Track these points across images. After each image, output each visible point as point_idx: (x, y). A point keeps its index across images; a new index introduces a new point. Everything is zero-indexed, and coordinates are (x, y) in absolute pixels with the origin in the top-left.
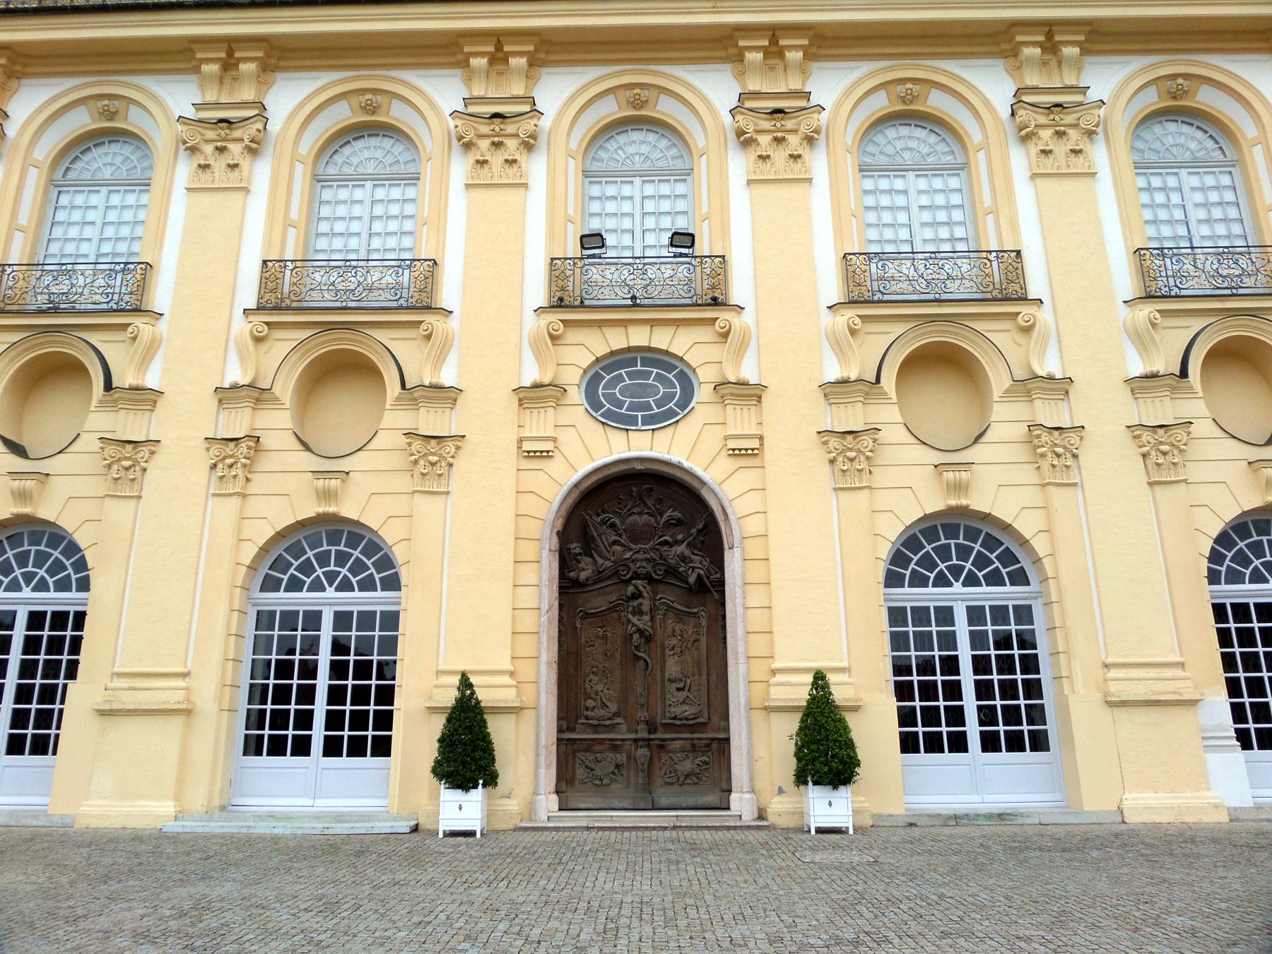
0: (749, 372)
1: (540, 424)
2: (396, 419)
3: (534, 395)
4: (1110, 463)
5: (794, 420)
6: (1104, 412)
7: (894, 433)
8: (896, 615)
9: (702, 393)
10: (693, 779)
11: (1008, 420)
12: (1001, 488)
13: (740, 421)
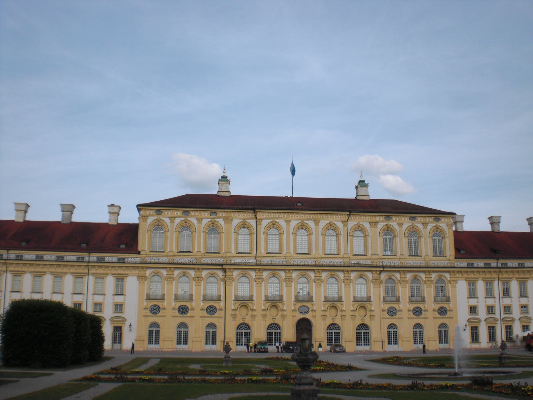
0: (314, 308)
1: (294, 313)
2: (280, 313)
3: (294, 310)
4: (348, 318)
5: (319, 314)
6: (348, 314)
8: (327, 333)
9: (310, 311)
11: (340, 314)
12: (338, 321)
13: (314, 314)
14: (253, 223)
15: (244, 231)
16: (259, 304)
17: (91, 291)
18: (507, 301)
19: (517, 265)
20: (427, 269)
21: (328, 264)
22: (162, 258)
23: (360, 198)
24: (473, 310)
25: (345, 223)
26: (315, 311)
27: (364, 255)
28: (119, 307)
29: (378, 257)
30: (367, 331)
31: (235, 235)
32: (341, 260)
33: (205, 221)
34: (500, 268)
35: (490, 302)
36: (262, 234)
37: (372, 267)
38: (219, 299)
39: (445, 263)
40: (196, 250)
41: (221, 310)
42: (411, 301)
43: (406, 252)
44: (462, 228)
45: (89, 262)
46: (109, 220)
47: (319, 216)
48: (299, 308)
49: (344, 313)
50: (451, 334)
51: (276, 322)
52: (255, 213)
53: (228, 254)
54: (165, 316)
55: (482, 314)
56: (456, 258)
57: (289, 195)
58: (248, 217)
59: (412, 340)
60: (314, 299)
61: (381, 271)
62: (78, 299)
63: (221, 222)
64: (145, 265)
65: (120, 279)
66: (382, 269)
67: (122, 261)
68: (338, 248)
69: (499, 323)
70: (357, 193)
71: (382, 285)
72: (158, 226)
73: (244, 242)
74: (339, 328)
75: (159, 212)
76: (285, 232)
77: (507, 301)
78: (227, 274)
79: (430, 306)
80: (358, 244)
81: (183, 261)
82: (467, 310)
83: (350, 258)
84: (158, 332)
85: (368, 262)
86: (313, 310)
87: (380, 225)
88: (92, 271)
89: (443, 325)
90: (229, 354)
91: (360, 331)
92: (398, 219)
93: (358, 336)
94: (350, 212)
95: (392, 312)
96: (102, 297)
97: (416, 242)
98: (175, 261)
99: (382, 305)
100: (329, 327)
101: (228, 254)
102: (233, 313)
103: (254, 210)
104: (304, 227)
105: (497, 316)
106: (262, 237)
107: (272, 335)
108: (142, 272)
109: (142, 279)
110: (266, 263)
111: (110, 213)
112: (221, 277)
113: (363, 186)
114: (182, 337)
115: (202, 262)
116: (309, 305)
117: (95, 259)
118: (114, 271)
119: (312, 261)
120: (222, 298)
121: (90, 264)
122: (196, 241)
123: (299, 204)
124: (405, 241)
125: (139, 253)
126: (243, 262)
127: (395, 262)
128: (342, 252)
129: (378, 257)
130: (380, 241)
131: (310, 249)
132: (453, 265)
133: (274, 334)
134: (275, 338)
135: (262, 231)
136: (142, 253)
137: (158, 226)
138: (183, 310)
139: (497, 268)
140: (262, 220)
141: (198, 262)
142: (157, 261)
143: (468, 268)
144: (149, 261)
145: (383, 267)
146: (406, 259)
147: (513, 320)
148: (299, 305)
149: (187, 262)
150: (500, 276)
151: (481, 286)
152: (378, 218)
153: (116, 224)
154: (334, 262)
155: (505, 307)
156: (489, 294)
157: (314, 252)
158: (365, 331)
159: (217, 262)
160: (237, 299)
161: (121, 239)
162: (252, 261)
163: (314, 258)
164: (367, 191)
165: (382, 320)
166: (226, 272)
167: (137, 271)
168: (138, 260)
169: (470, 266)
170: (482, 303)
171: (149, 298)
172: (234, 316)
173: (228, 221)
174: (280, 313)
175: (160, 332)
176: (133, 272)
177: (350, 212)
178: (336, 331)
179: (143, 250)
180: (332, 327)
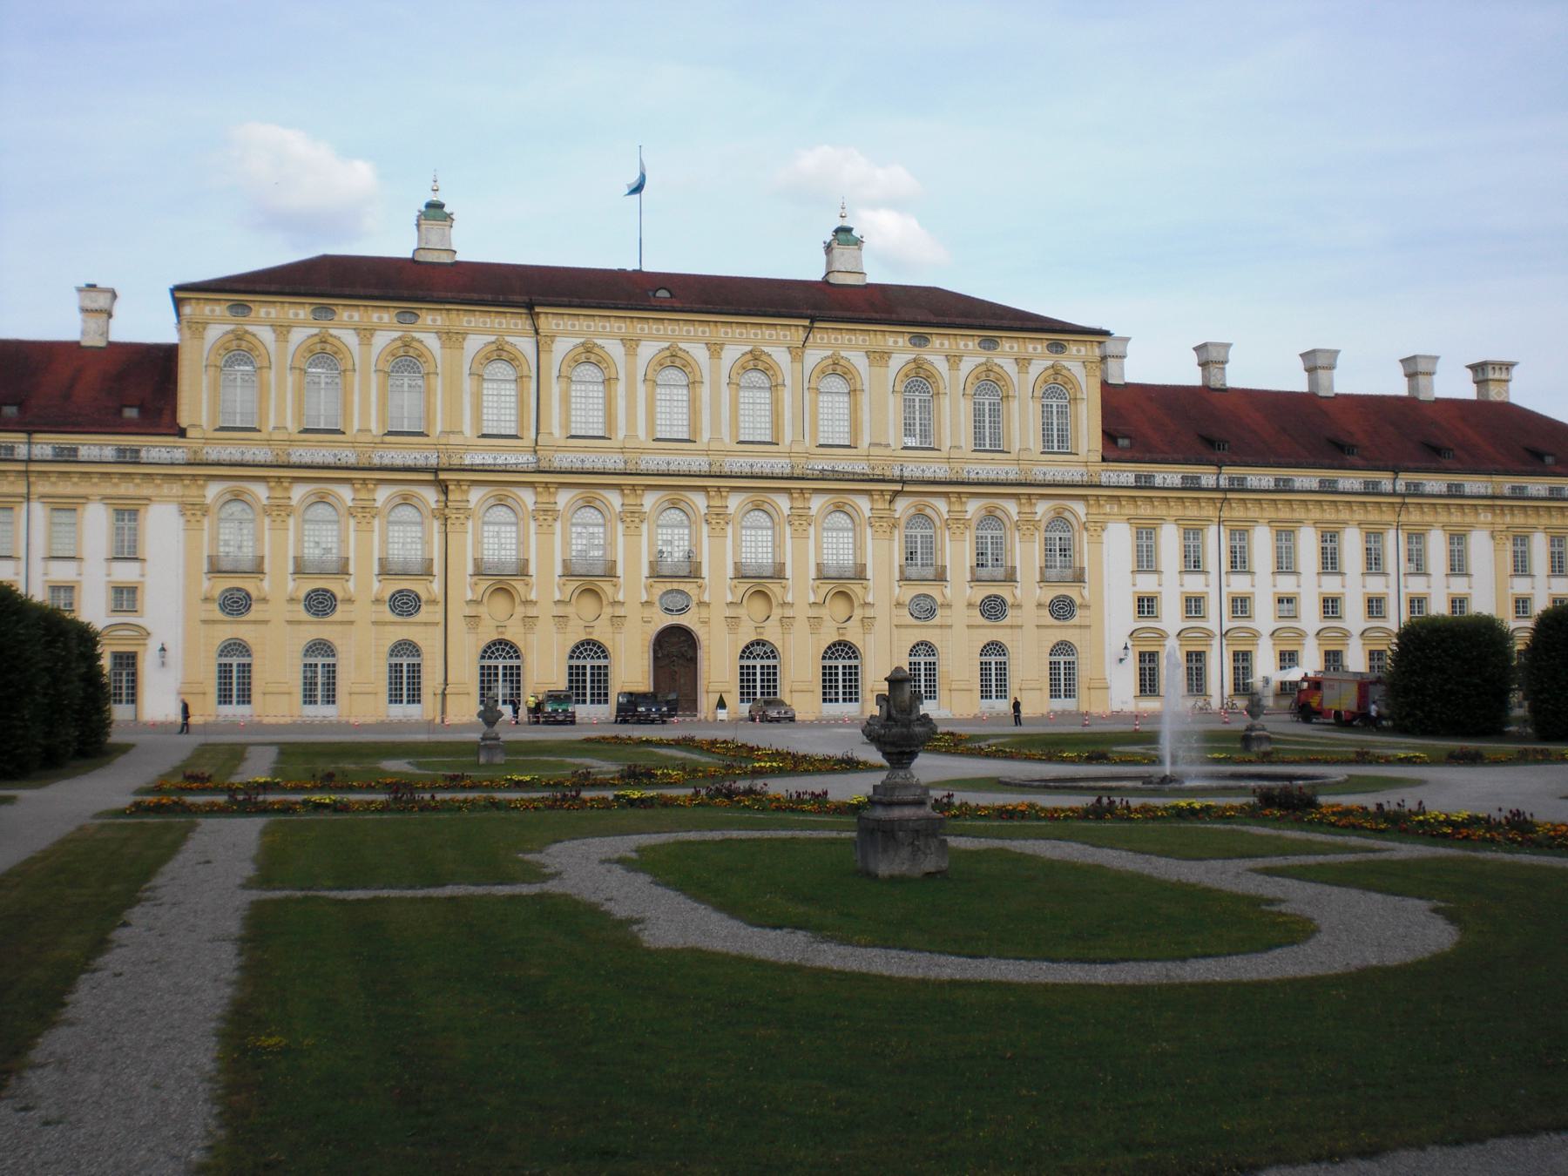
0: (706, 598)
1: (647, 612)
2: (608, 611)
3: (648, 603)
4: (801, 626)
5: (718, 613)
6: (801, 613)
7: (745, 618)
9: (693, 605)
10: (687, 709)
11: (777, 612)
12: (772, 634)
13: (704, 613)
14: (526, 345)
15: (501, 369)
16: (546, 587)
17: (39, 550)
18: (1239, 584)
19: (1444, 489)
20: (1025, 488)
21: (747, 470)
22: (254, 450)
23: (837, 279)
24: (1146, 605)
25: (797, 353)
26: (708, 605)
27: (849, 447)
29: (887, 452)
30: (853, 662)
31: (474, 383)
32: (784, 461)
33: (382, 340)
34: (1225, 491)
35: (1194, 584)
36: (554, 380)
37: (871, 480)
38: (427, 572)
39: (1074, 473)
40: (356, 426)
41: (434, 602)
42: (975, 580)
43: (966, 439)
44: (1122, 376)
45: (30, 461)
46: (83, 333)
47: (722, 330)
48: (661, 597)
49: (788, 612)
50: (1083, 673)
51: (595, 637)
52: (533, 316)
53: (453, 439)
54: (266, 622)
55: (1171, 617)
56: (1104, 460)
57: (631, 265)
58: (512, 329)
59: (976, 686)
60: (705, 572)
61: (896, 493)
62: (63, 572)
63: (432, 342)
64: (200, 469)
65: (127, 513)
66: (898, 487)
67: (129, 457)
68: (776, 425)
69: (1216, 642)
70: (829, 263)
71: (896, 532)
72: (240, 351)
73: (500, 404)
74: (773, 654)
75: (241, 309)
76: (622, 375)
77: (1239, 584)
78: (451, 497)
79: (1029, 593)
80: (833, 415)
81: (318, 459)
82: (1131, 606)
83: (808, 455)
84: (246, 669)
85: (860, 467)
86: (700, 604)
87: (898, 361)
88: (41, 487)
89: (1063, 647)
90: (497, 728)
91: (833, 663)
92: (946, 343)
93: (828, 675)
94: (813, 320)
95: (925, 610)
96: (72, 565)
97: (995, 411)
98: (294, 459)
99: (897, 590)
100: (747, 652)
101: (453, 439)
102: (469, 611)
103: (530, 306)
104: (678, 363)
105: (1212, 624)
106: (555, 389)
107: (584, 674)
108: (194, 491)
109: (193, 511)
110: (566, 465)
111: (84, 310)
112: (434, 506)
113: (847, 243)
114: (320, 681)
115: (376, 461)
116: (688, 587)
117: (48, 452)
118: (108, 489)
119: (699, 463)
120: (437, 568)
121: (33, 467)
122: (356, 398)
123: (663, 294)
124: (966, 408)
125: (182, 433)
126: (499, 461)
127: (935, 467)
128: (787, 436)
129: (887, 452)
130: (894, 408)
131: (694, 424)
132: (1095, 480)
133: (588, 671)
134: (592, 681)
135: (555, 373)
136: (190, 433)
137: (240, 351)
138: (321, 603)
139: (1217, 489)
140: (552, 337)
141: (364, 462)
142: (237, 457)
143: (1183, 489)
144: (213, 457)
145: (903, 481)
146: (967, 461)
147: (1255, 635)
148: (661, 588)
149: (330, 460)
150: (1225, 514)
151: (1170, 540)
152: (890, 340)
153: (102, 344)
154: (765, 464)
155: (1234, 600)
156: (1193, 563)
157: (705, 436)
158: (847, 663)
159: (421, 462)
160: (480, 572)
161: (124, 391)
162: (525, 459)
163: (707, 452)
164: (859, 260)
165: (895, 631)
166: (446, 492)
167: (176, 489)
168: (179, 455)
169: (1144, 483)
170: (1171, 586)
171: (215, 570)
172: (473, 619)
173: (451, 338)
174: (608, 611)
175: (253, 668)
176: (165, 490)
177: (813, 320)
178: (766, 662)
179: (194, 426)
180: (758, 650)
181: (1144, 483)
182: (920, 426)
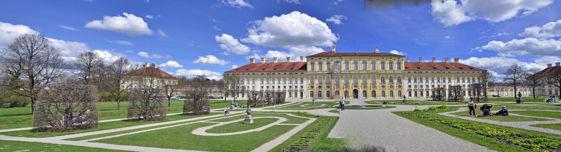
24: (410, 86)
28: (302, 87)
55: (413, 88)
181: (409, 72)
182: (383, 68)
